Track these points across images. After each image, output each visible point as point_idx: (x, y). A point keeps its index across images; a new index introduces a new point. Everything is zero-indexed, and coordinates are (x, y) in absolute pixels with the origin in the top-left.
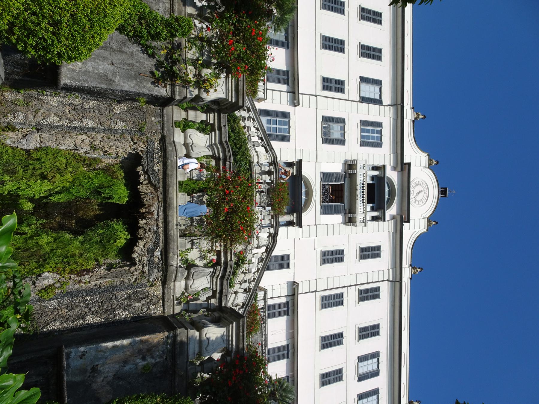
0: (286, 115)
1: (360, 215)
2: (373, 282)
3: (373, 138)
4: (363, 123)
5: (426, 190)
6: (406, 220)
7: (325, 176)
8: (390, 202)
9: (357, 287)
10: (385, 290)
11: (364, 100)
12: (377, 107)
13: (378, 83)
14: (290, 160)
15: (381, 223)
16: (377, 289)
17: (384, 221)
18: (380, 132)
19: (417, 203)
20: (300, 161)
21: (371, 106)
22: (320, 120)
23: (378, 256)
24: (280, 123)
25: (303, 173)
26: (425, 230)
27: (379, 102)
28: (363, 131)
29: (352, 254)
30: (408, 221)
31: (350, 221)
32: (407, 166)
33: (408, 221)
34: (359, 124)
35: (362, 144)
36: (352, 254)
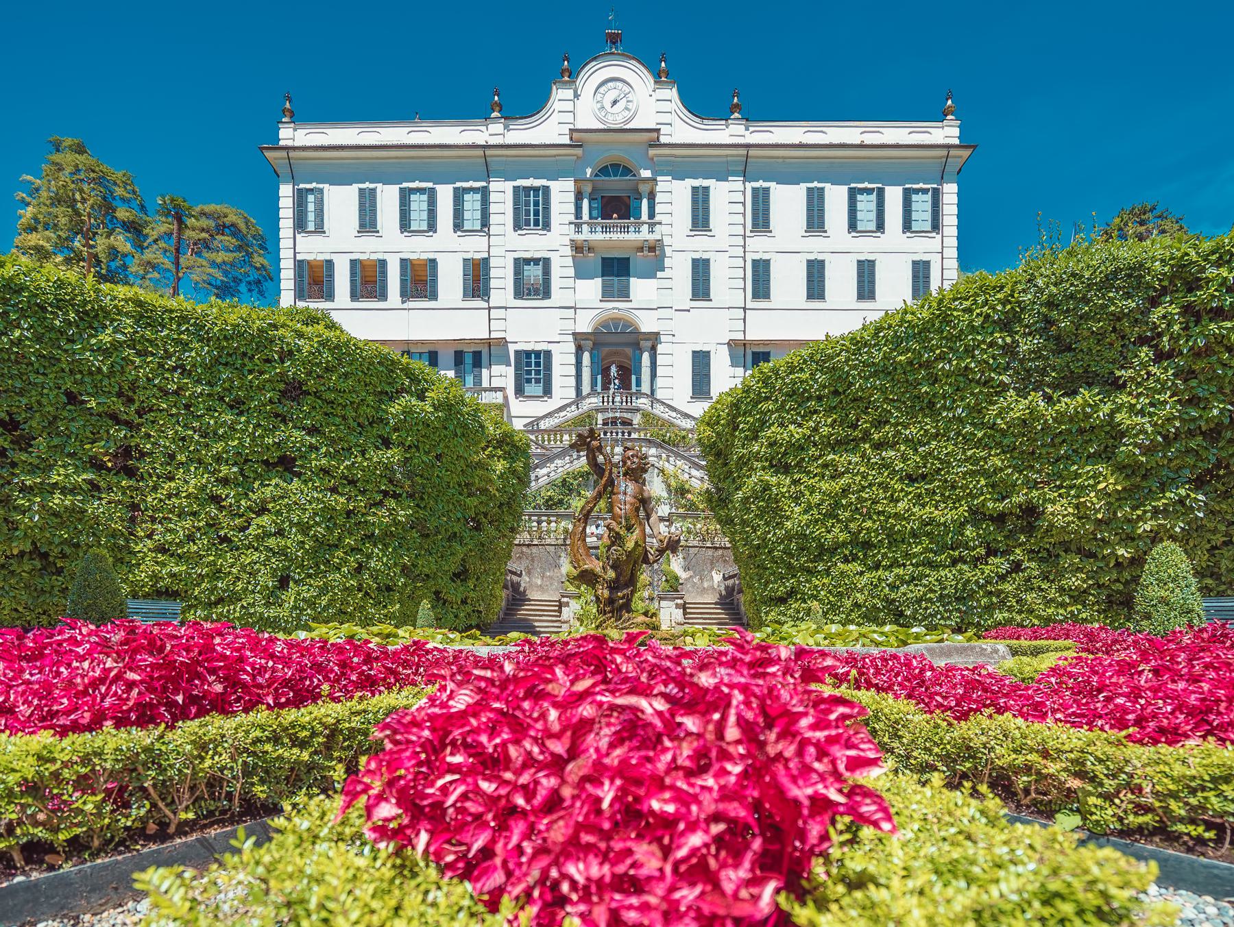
1: (644, 234)
4: (517, 226)
5: (611, 84)
6: (655, 135)
9: (748, 233)
11: (485, 223)
14: (572, 348)
18: (527, 190)
19: (630, 106)
21: (493, 208)
23: (706, 189)
27: (485, 192)
28: (527, 223)
29: (701, 245)
30: (658, 130)
32: (575, 135)
33: (658, 130)
35: (547, 226)
36: (701, 245)
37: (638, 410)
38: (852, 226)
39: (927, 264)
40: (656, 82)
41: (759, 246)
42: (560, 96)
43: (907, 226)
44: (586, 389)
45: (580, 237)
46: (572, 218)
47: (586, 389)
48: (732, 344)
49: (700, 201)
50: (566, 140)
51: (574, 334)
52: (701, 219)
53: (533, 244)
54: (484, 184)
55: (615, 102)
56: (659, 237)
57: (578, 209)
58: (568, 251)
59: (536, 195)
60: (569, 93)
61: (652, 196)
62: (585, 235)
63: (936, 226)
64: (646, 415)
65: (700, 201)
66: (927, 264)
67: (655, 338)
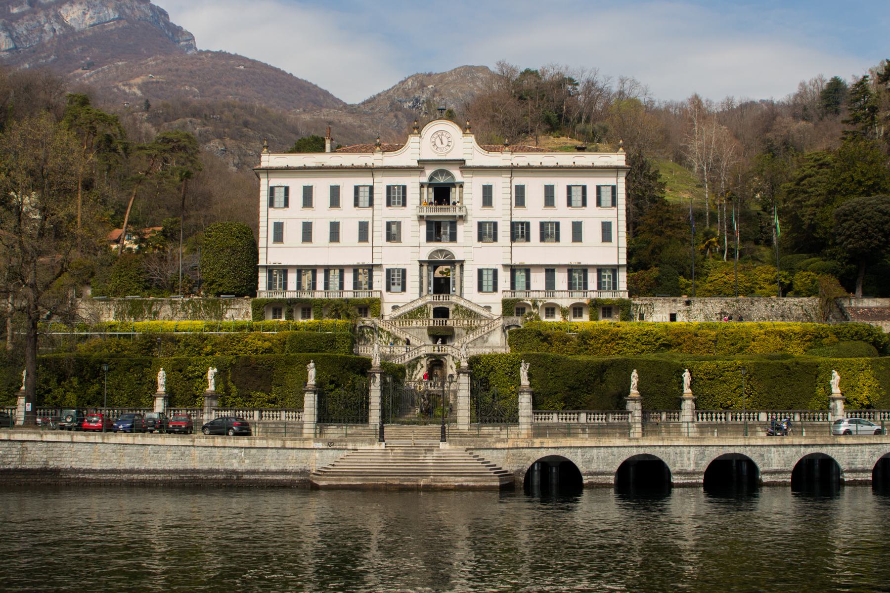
0: (388, 271)
2: (511, 193)
3: (399, 193)
4: (389, 204)
7: (429, 239)
8: (448, 174)
9: (513, 208)
10: (518, 181)
11: (371, 204)
12: (375, 191)
13: (357, 189)
15: (465, 186)
16: (516, 187)
17: (463, 183)
19: (450, 144)
20: (420, 261)
21: (375, 196)
22: (389, 244)
24: (394, 275)
25: (427, 259)
26: (473, 136)
27: (371, 188)
28: (394, 204)
29: (487, 215)
30: (464, 161)
31: (461, 217)
33: (464, 161)
34: (390, 208)
35: (404, 205)
37: (452, 303)
38: (569, 204)
39: (610, 223)
40: (464, 133)
41: (520, 215)
42: (413, 140)
43: (599, 203)
44: (425, 293)
45: (422, 214)
46: (418, 202)
47: (425, 293)
48: (505, 266)
49: (487, 191)
50: (415, 164)
51: (420, 261)
52: (487, 201)
53: (395, 213)
54: (371, 184)
55: (442, 143)
56: (463, 213)
57: (421, 194)
58: (416, 218)
59: (399, 189)
60: (417, 138)
61: (461, 185)
62: (425, 213)
63: (614, 203)
64: (456, 305)
65: (487, 191)
66: (610, 223)
67: (462, 263)
